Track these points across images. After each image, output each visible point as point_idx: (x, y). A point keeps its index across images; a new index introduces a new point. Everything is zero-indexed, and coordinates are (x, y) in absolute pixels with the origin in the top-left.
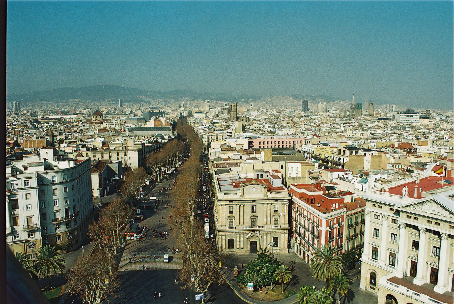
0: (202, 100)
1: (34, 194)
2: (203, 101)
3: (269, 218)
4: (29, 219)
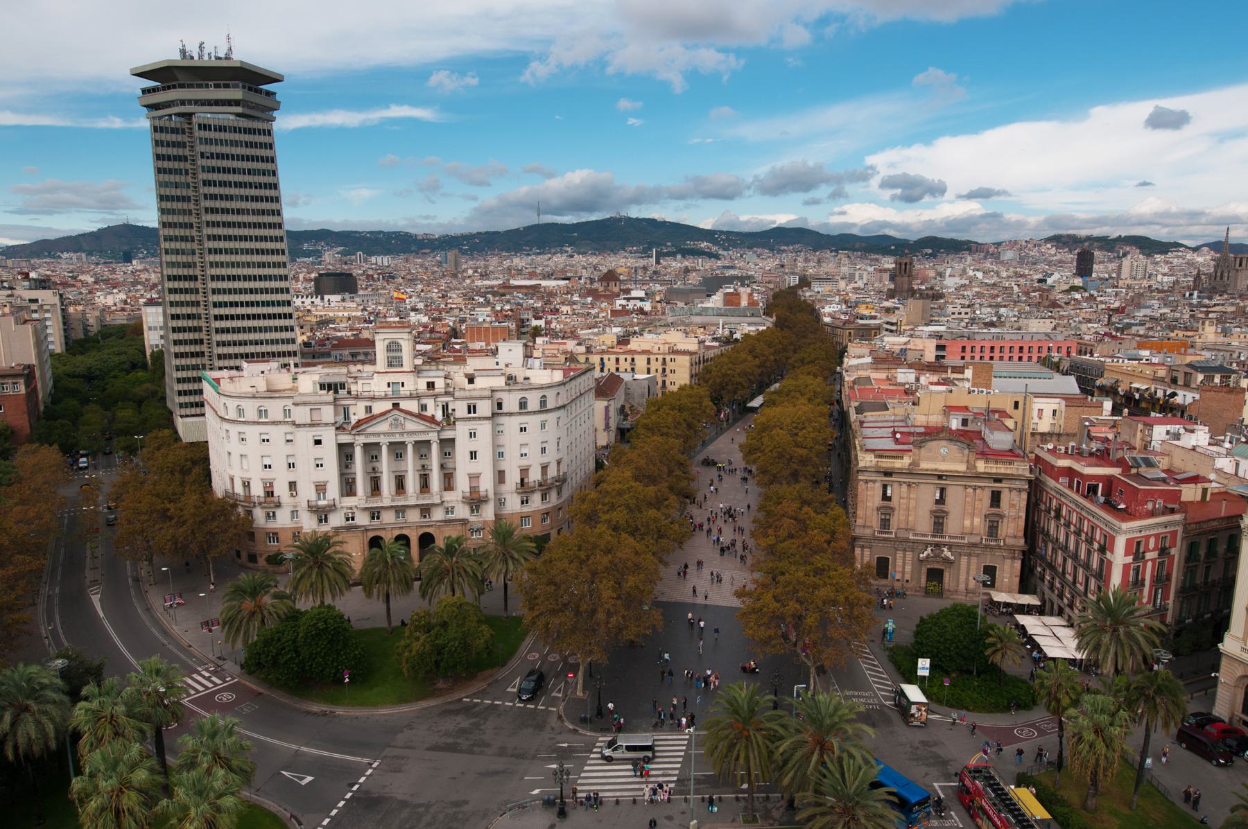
1: (484, 429)
3: (977, 521)
4: (474, 477)
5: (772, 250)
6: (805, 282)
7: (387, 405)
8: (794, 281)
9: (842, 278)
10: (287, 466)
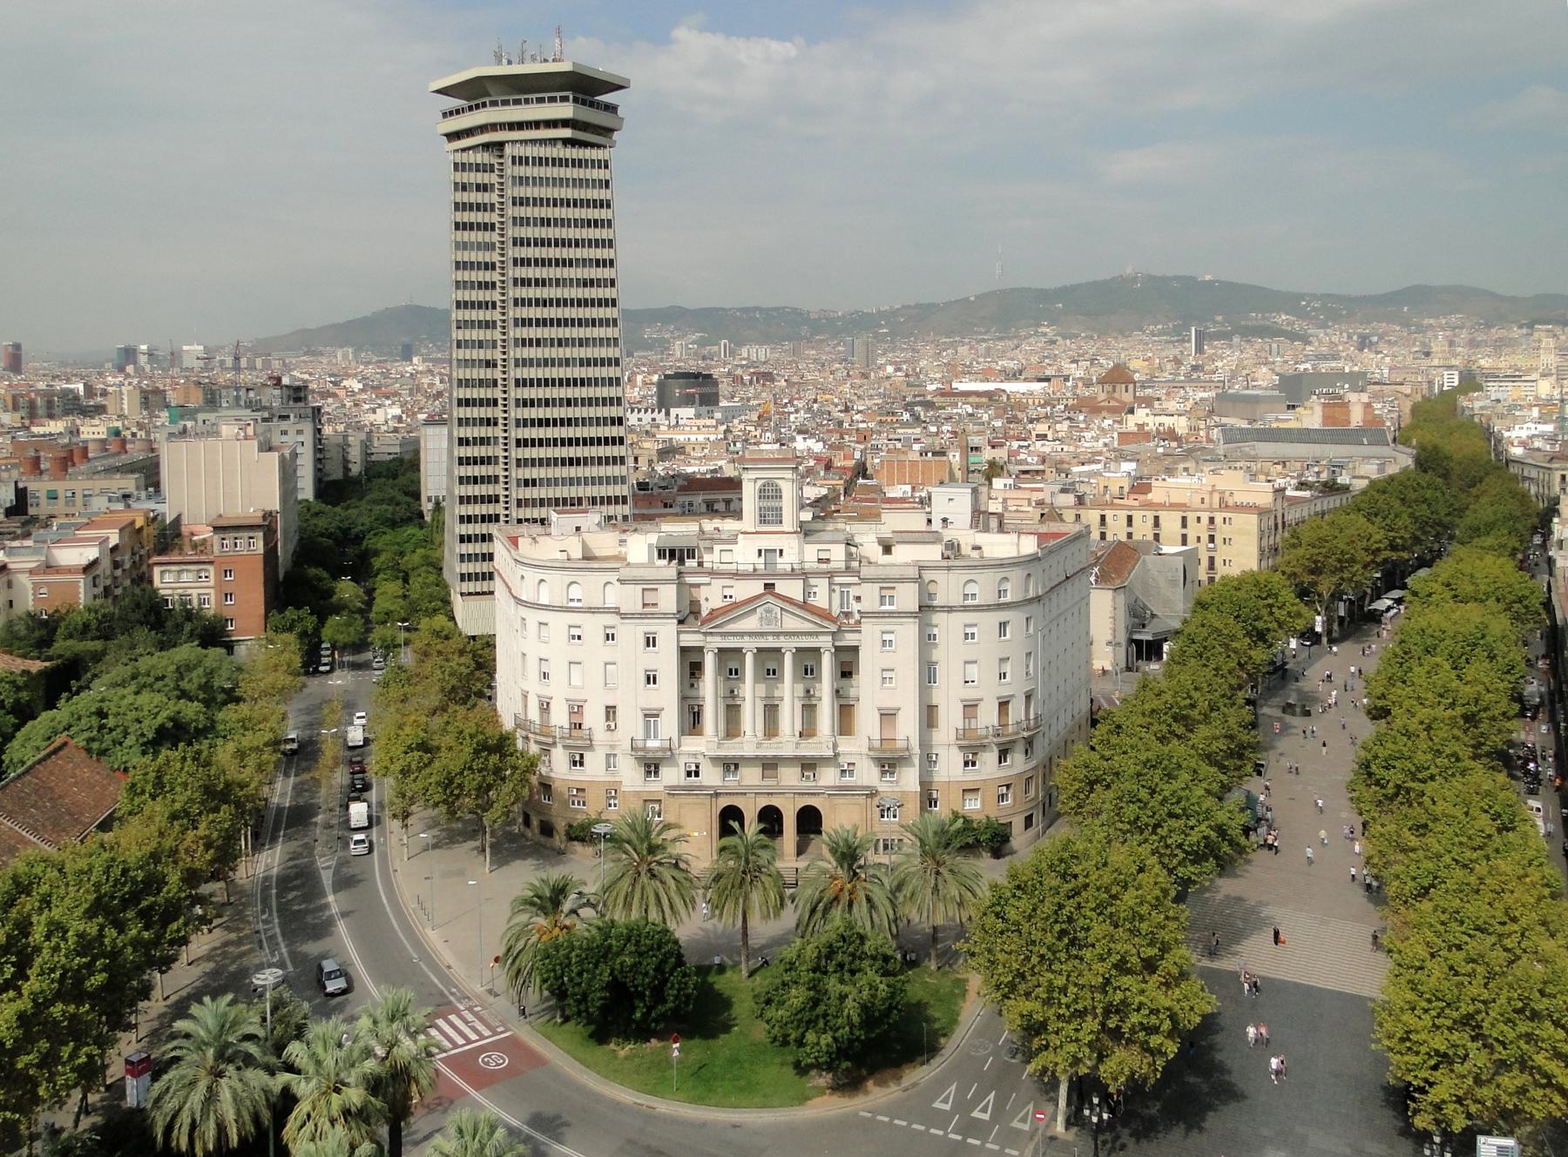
0: (1520, 327)
2: (1524, 331)
4: (888, 716)
5: (1406, 324)
6: (1471, 382)
7: (757, 587)
8: (1451, 380)
9: (1544, 375)
10: (603, 637)
